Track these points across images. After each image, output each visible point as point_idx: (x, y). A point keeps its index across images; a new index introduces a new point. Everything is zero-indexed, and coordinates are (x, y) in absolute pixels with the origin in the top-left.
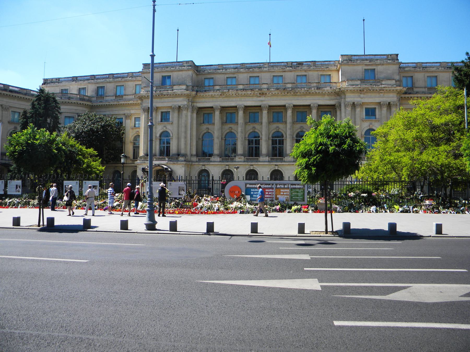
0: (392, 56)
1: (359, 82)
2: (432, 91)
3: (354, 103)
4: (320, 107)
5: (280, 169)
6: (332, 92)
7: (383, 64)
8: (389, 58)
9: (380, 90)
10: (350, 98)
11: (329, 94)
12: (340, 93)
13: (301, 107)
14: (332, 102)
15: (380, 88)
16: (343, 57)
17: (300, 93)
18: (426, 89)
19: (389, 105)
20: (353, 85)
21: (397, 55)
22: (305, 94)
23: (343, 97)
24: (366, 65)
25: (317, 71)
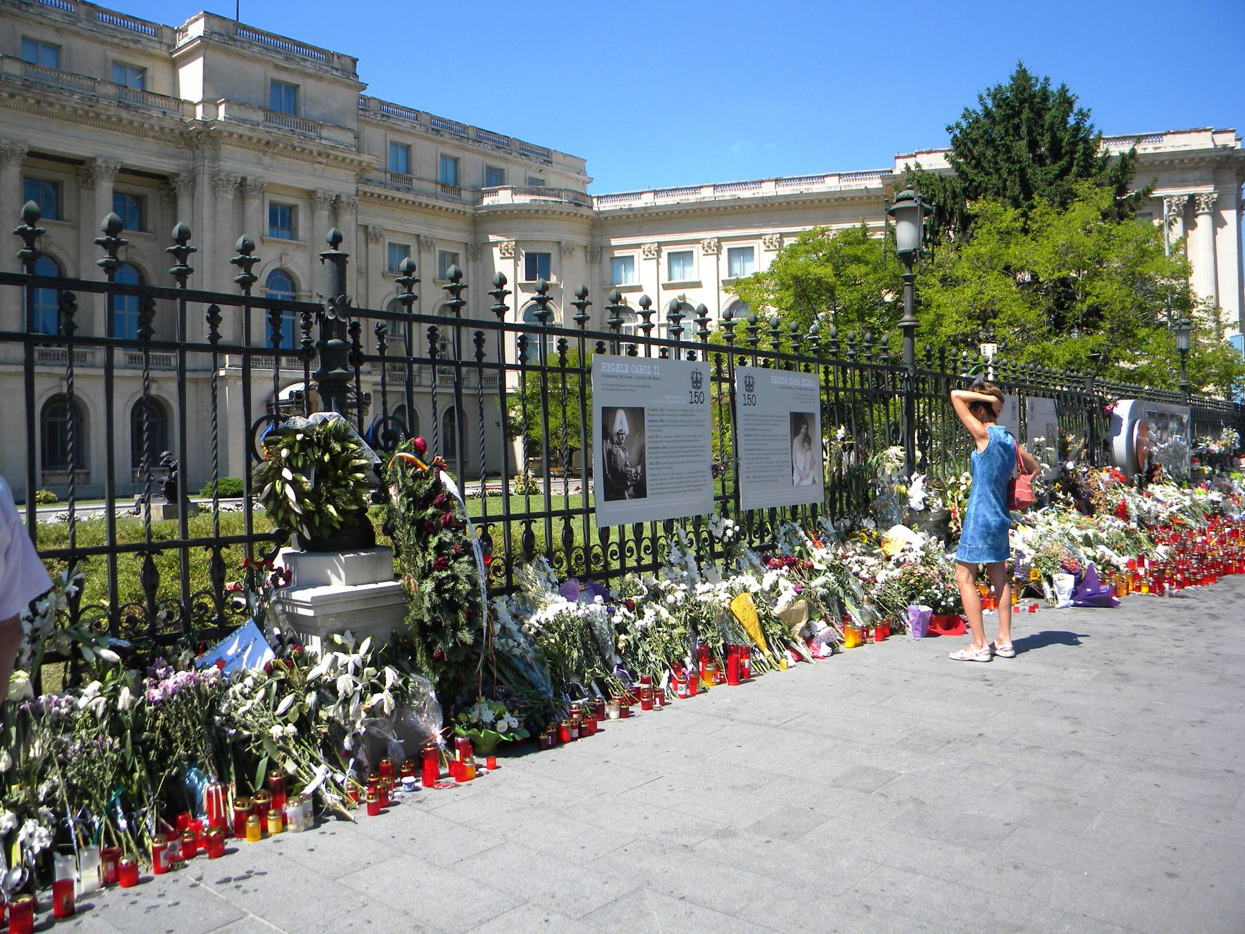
0: (343, 60)
1: (259, 116)
2: (400, 185)
3: (244, 179)
6: (172, 130)
7: (321, 79)
8: (336, 65)
10: (235, 161)
11: (161, 135)
12: (200, 139)
13: (44, 163)
14: (165, 165)
15: (321, 149)
16: (211, 20)
17: (63, 107)
18: (389, 176)
19: (336, 205)
20: (244, 121)
21: (355, 61)
22: (76, 117)
24: (277, 66)
25: (103, 43)
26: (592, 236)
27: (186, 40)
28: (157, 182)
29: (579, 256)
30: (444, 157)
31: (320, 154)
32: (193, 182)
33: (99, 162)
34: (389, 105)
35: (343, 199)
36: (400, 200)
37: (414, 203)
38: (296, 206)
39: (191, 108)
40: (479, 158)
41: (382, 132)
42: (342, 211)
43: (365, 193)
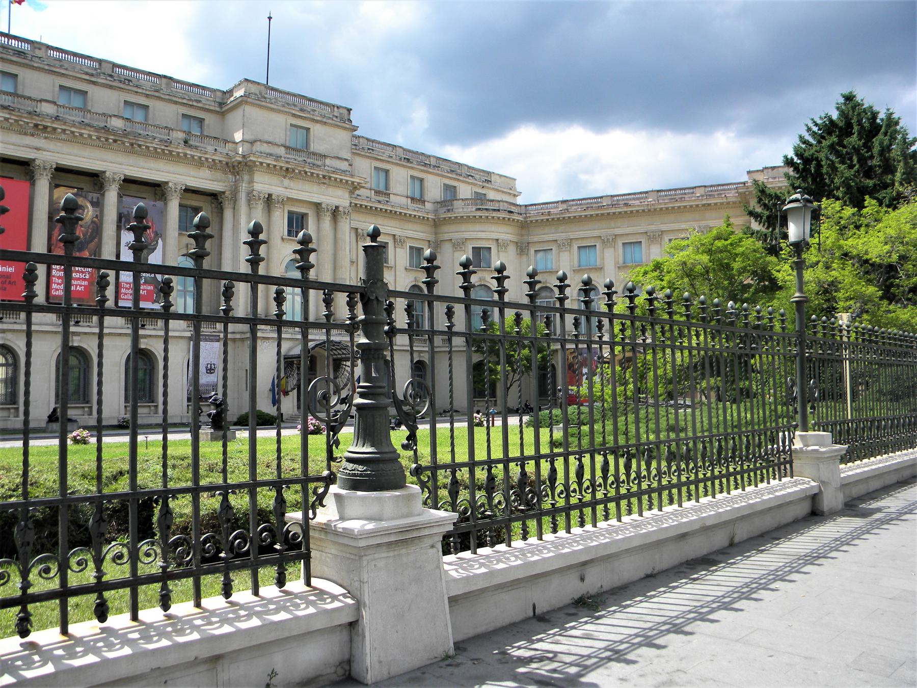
1: (281, 151)
3: (270, 195)
4: (189, 195)
5: (85, 346)
9: (324, 177)
10: (264, 183)
11: (213, 165)
19: (335, 213)
21: (349, 110)
22: (156, 155)
23: (246, 177)
24: (294, 115)
26: (522, 235)
27: (232, 99)
28: (209, 198)
29: (512, 249)
30: (412, 177)
31: (324, 177)
32: (235, 200)
33: (170, 185)
34: (373, 141)
35: (341, 209)
36: (381, 209)
37: (391, 211)
38: (307, 214)
39: (234, 145)
40: (438, 179)
41: (368, 161)
42: (339, 217)
43: (356, 205)
